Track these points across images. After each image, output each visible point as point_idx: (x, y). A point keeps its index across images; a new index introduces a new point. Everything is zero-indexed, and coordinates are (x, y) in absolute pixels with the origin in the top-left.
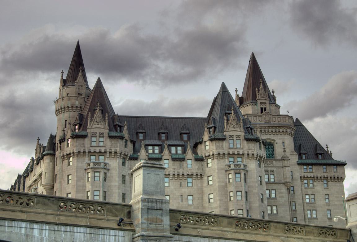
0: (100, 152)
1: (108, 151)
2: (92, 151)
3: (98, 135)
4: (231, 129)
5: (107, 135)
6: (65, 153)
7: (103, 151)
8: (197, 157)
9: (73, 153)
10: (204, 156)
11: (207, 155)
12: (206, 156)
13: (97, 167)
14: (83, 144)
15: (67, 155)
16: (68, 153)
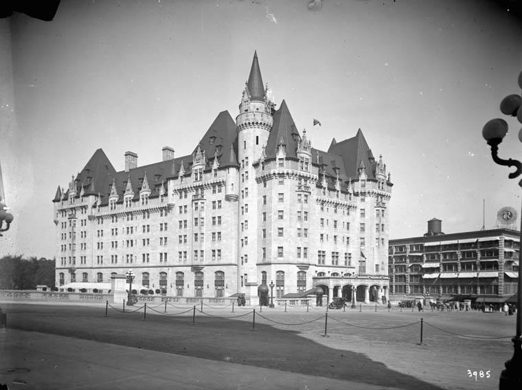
0: (306, 177)
6: (277, 172)
15: (279, 174)
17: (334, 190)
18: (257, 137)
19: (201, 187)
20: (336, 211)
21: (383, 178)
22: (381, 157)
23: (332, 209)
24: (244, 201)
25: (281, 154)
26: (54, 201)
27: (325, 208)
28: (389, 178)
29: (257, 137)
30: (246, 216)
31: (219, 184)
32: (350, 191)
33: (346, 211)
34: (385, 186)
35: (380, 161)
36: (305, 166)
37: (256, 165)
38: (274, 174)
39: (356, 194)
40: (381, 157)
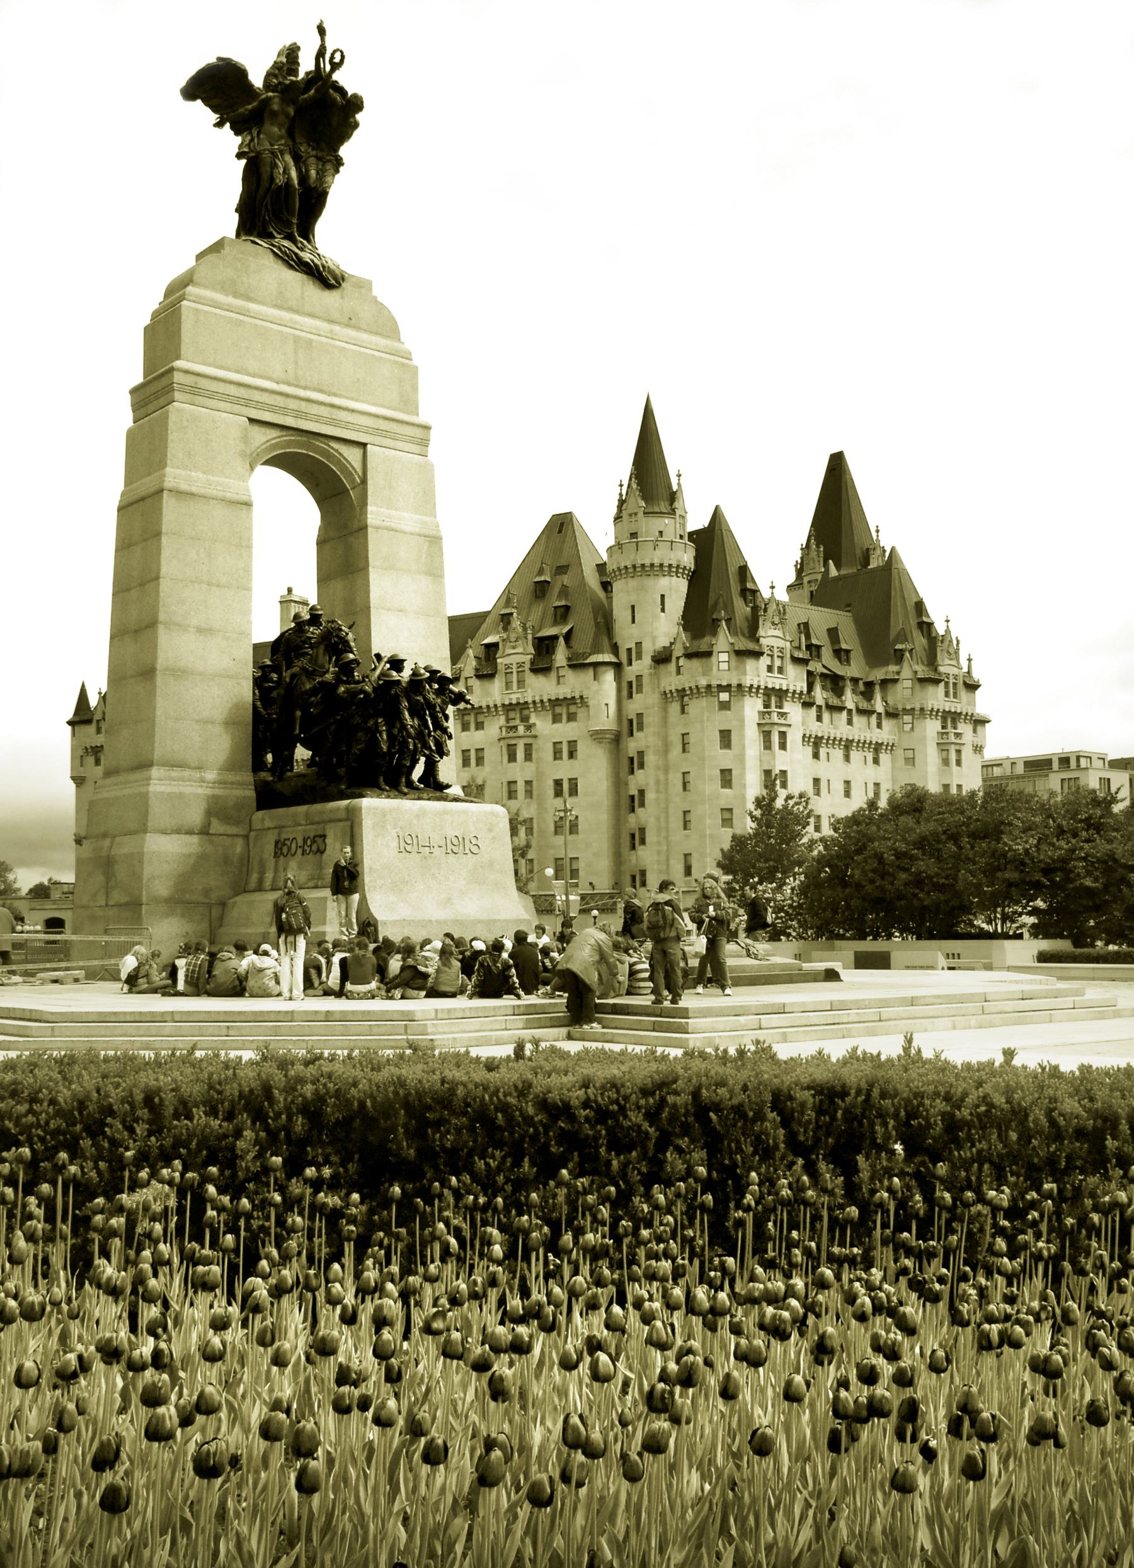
1: (791, 689)
2: (770, 686)
3: (776, 650)
4: (948, 662)
5: (788, 656)
6: (714, 683)
7: (784, 688)
8: (891, 710)
9: (739, 686)
10: (900, 707)
11: (908, 707)
12: (904, 709)
13: (782, 721)
14: (757, 669)
15: (719, 686)
16: (724, 683)
17: (840, 709)
18: (663, 596)
19: (522, 706)
20: (847, 758)
21: (955, 671)
22: (948, 621)
23: (838, 753)
24: (632, 746)
25: (723, 641)
26: (69, 723)
27: (823, 751)
28: (969, 667)
29: (663, 596)
30: (640, 779)
31: (570, 701)
32: (879, 707)
33: (870, 757)
34: (963, 693)
35: (948, 631)
36: (778, 663)
37: (662, 658)
38: (709, 686)
39: (892, 714)
40: (948, 621)
